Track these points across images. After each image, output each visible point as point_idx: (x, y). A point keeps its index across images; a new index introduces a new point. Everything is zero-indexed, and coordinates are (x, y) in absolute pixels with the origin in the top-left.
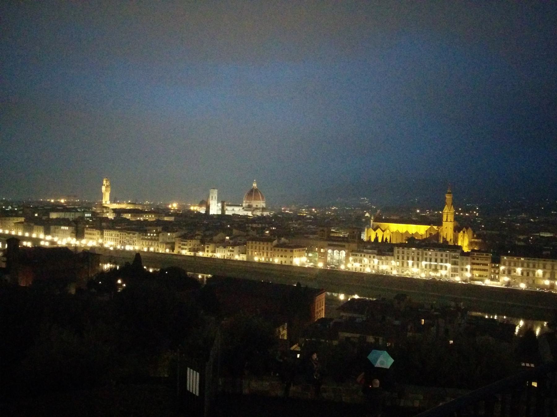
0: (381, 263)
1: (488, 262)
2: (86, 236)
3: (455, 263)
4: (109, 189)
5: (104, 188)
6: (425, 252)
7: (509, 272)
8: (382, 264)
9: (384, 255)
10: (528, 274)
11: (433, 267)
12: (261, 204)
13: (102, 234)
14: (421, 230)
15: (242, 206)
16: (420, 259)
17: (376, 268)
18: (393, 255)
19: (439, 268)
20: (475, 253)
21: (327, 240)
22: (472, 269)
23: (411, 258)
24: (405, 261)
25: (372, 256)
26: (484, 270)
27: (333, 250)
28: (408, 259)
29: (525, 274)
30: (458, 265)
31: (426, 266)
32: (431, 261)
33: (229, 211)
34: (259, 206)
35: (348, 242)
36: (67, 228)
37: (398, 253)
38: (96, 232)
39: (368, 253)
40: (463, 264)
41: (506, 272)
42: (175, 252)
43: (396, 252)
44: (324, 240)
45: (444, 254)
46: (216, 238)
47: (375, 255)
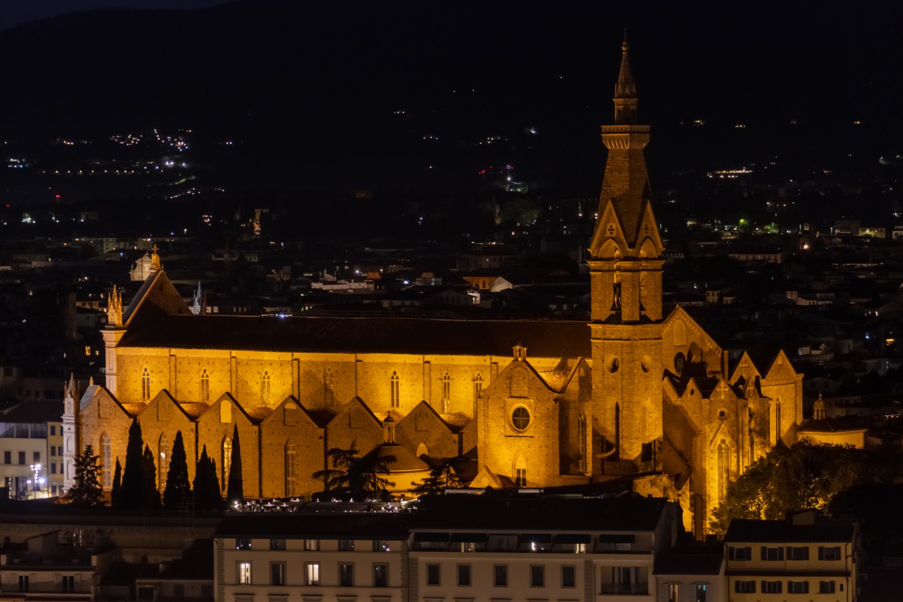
20: (756, 548)
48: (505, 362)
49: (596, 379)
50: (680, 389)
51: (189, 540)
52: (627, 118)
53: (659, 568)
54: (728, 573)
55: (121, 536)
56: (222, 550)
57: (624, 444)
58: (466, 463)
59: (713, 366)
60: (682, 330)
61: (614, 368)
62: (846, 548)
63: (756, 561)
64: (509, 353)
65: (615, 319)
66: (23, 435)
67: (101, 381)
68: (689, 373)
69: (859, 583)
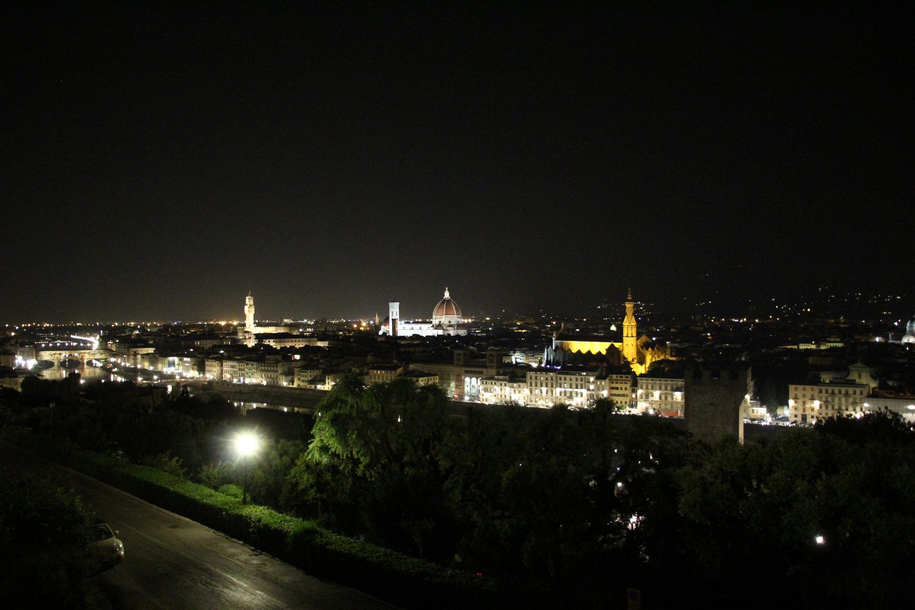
1: (628, 386)
2: (207, 368)
4: (253, 309)
5: (246, 308)
7: (647, 396)
9: (516, 382)
11: (568, 394)
12: (455, 319)
13: (222, 365)
14: (599, 347)
15: (431, 322)
19: (574, 395)
23: (544, 384)
25: (503, 383)
26: (623, 395)
27: (471, 378)
29: (663, 398)
33: (406, 330)
34: (452, 323)
35: (485, 367)
36: (189, 359)
38: (216, 363)
39: (498, 380)
42: (295, 385)
46: (342, 368)
52: (629, 301)
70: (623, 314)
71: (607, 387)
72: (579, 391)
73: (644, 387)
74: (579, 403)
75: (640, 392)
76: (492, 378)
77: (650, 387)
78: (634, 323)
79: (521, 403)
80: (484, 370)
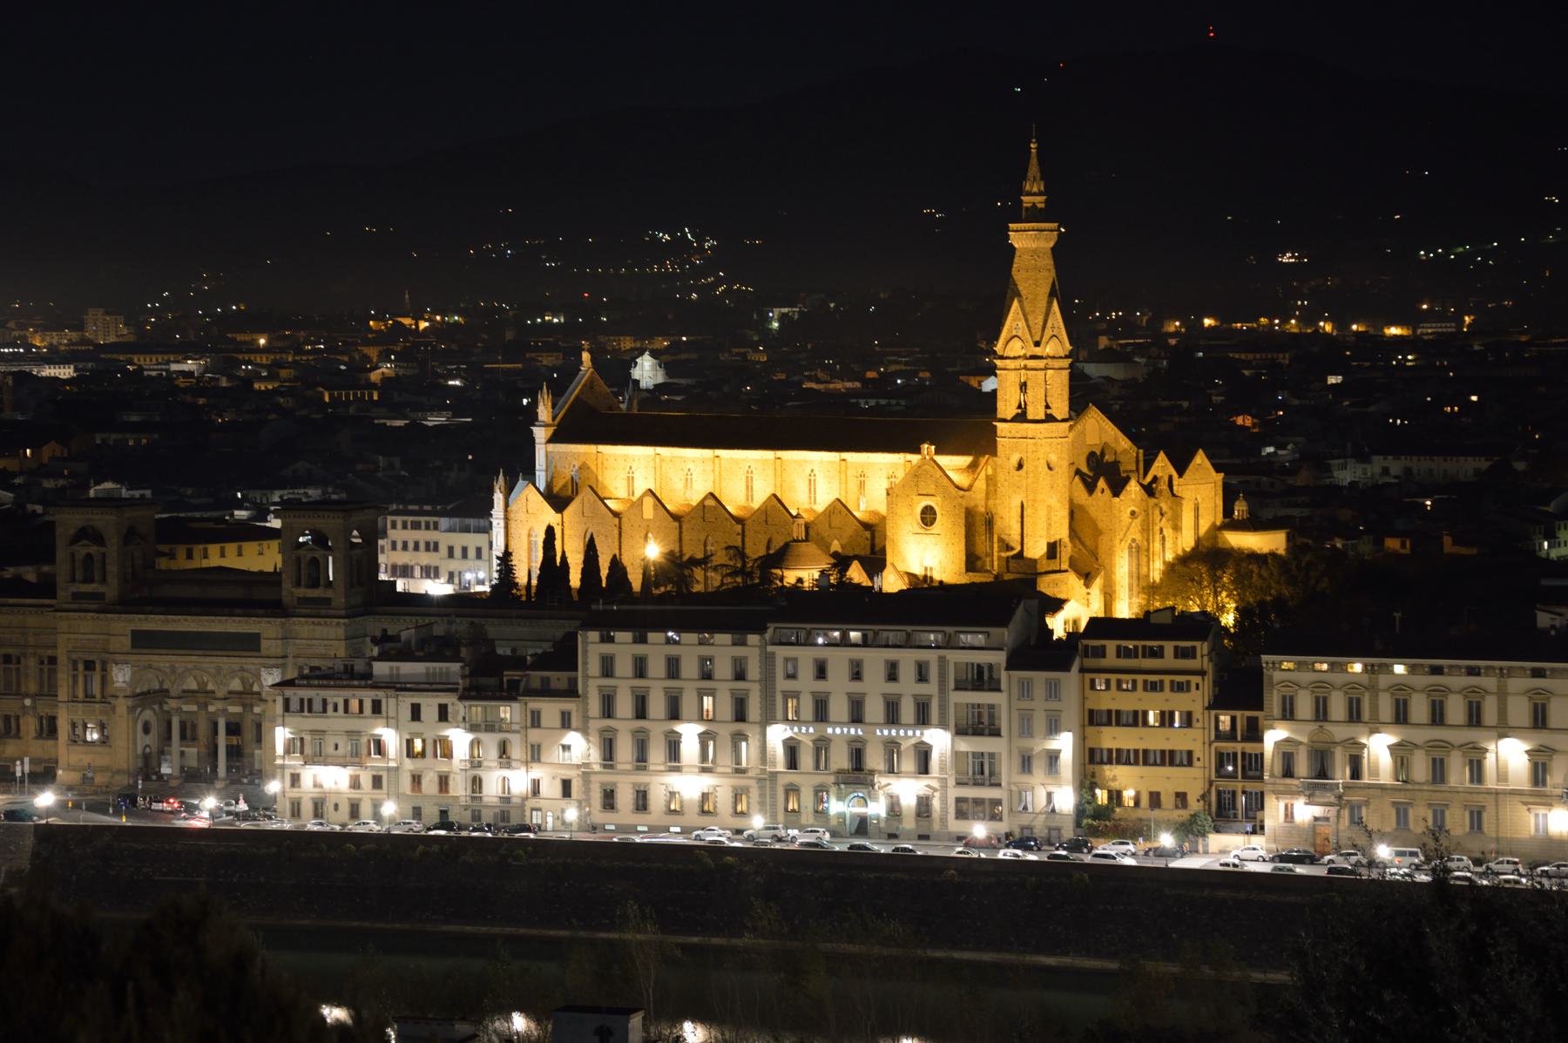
0: (490, 753)
1: (1196, 699)
3: (976, 725)
6: (782, 652)
8: (503, 750)
10: (1439, 771)
11: (840, 759)
16: (754, 709)
17: (459, 788)
18: (571, 692)
19: (874, 759)
20: (1111, 646)
21: (128, 604)
22: (1092, 759)
24: (656, 729)
25: (430, 705)
26: (1168, 758)
28: (675, 714)
29: (1420, 769)
30: (996, 733)
31: (792, 749)
32: (821, 714)
35: (277, 609)
37: (608, 668)
39: (397, 686)
40: (1027, 730)
41: (1302, 766)
43: (594, 667)
44: (105, 607)
45: (907, 659)
47: (450, 700)
48: (915, 458)
49: (1001, 477)
50: (1090, 488)
51: (559, 634)
52: (1034, 215)
53: (1011, 665)
54: (1082, 670)
55: (493, 629)
56: (585, 643)
57: (1028, 542)
58: (875, 562)
59: (1128, 464)
60: (1098, 429)
61: (1020, 466)
62: (1202, 647)
63: (1111, 659)
64: (917, 451)
65: (1021, 417)
66: (466, 530)
67: (530, 475)
68: (1100, 472)
69: (1216, 683)
70: (995, 297)
71: (1070, 706)
72: (909, 736)
73: (1305, 706)
74: (908, 802)
75: (1274, 736)
76: (353, 676)
77: (1338, 707)
78: (1057, 345)
79: (561, 819)
80: (267, 628)
